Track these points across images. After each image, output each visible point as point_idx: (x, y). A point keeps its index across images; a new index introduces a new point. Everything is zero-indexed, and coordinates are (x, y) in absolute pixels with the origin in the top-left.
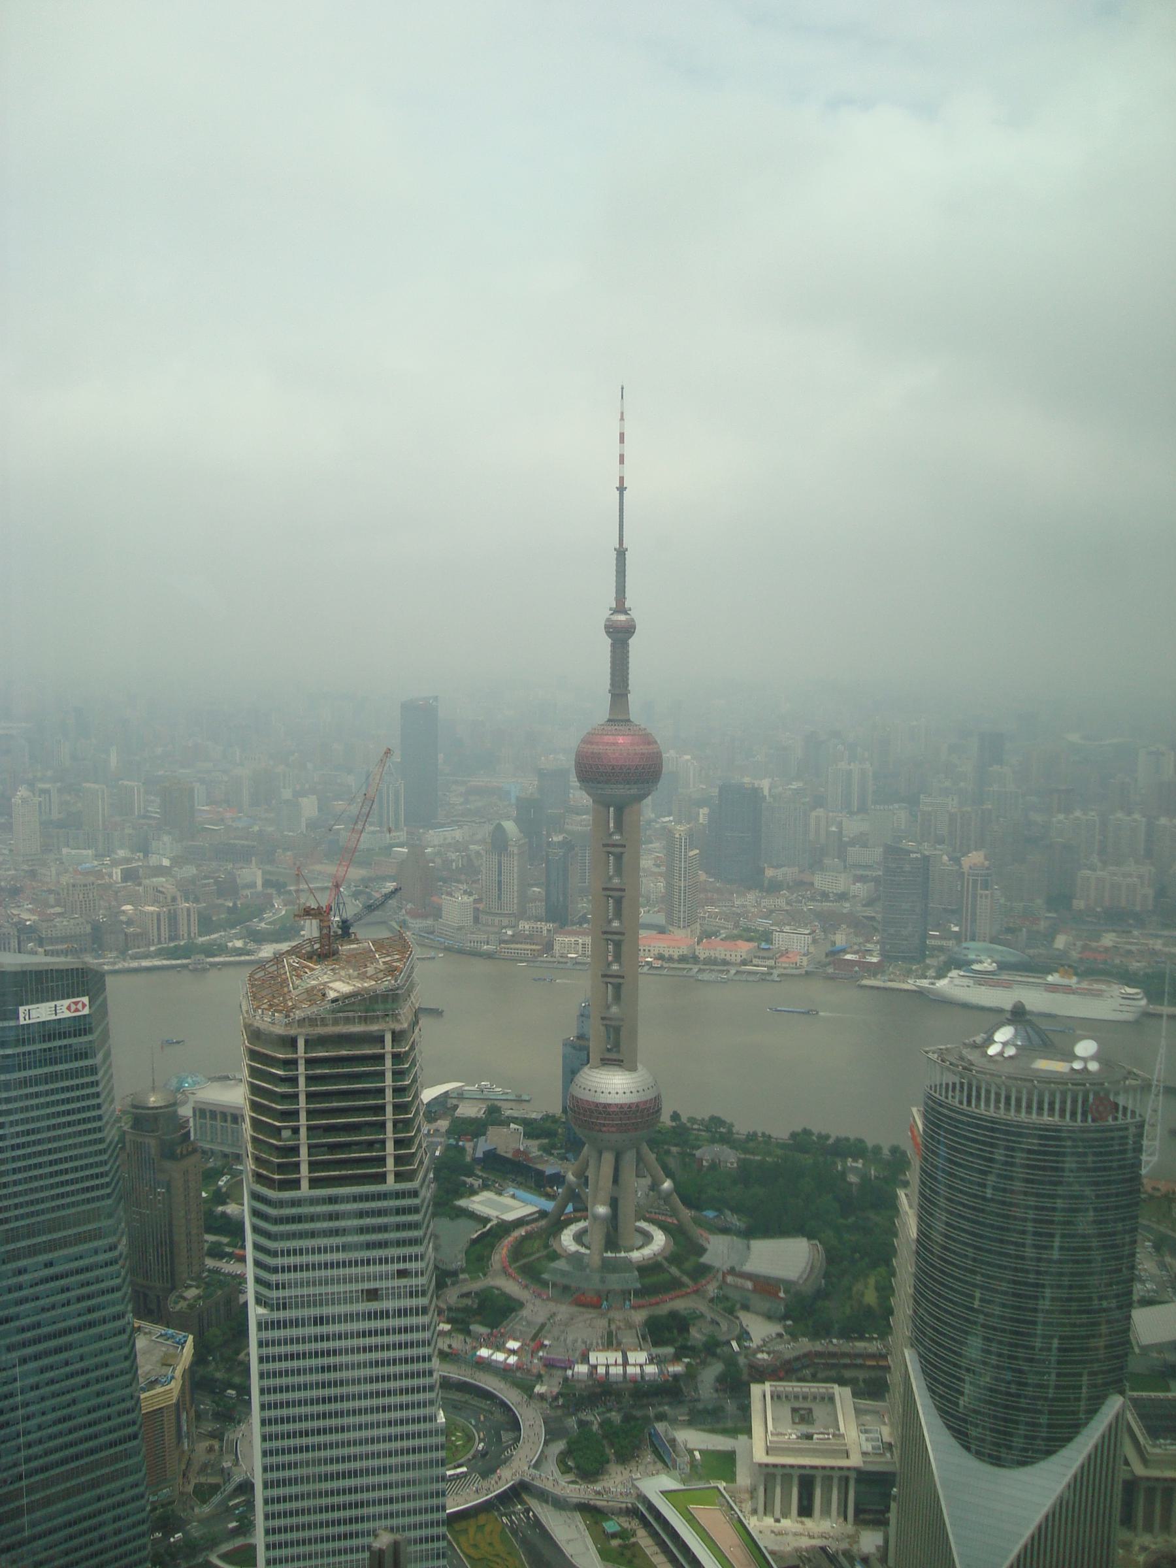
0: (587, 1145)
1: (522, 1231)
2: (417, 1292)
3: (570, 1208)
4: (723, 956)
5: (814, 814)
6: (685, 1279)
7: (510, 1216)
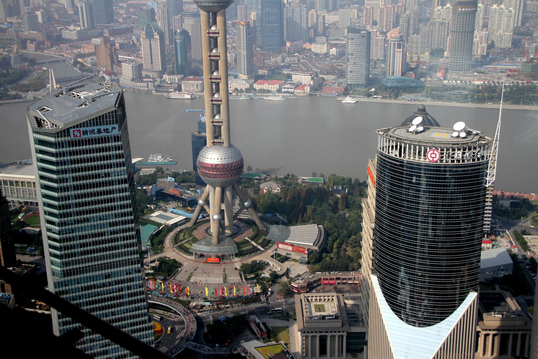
0: (208, 185)
1: (178, 229)
2: (135, 261)
3: (201, 217)
4: (267, 88)
5: (310, 12)
6: (259, 247)
7: (171, 222)
